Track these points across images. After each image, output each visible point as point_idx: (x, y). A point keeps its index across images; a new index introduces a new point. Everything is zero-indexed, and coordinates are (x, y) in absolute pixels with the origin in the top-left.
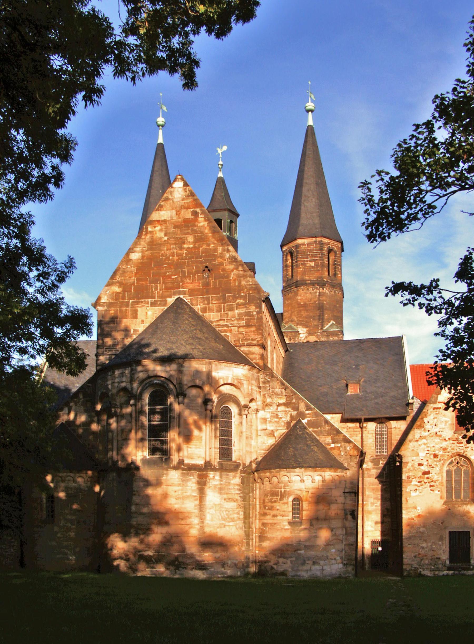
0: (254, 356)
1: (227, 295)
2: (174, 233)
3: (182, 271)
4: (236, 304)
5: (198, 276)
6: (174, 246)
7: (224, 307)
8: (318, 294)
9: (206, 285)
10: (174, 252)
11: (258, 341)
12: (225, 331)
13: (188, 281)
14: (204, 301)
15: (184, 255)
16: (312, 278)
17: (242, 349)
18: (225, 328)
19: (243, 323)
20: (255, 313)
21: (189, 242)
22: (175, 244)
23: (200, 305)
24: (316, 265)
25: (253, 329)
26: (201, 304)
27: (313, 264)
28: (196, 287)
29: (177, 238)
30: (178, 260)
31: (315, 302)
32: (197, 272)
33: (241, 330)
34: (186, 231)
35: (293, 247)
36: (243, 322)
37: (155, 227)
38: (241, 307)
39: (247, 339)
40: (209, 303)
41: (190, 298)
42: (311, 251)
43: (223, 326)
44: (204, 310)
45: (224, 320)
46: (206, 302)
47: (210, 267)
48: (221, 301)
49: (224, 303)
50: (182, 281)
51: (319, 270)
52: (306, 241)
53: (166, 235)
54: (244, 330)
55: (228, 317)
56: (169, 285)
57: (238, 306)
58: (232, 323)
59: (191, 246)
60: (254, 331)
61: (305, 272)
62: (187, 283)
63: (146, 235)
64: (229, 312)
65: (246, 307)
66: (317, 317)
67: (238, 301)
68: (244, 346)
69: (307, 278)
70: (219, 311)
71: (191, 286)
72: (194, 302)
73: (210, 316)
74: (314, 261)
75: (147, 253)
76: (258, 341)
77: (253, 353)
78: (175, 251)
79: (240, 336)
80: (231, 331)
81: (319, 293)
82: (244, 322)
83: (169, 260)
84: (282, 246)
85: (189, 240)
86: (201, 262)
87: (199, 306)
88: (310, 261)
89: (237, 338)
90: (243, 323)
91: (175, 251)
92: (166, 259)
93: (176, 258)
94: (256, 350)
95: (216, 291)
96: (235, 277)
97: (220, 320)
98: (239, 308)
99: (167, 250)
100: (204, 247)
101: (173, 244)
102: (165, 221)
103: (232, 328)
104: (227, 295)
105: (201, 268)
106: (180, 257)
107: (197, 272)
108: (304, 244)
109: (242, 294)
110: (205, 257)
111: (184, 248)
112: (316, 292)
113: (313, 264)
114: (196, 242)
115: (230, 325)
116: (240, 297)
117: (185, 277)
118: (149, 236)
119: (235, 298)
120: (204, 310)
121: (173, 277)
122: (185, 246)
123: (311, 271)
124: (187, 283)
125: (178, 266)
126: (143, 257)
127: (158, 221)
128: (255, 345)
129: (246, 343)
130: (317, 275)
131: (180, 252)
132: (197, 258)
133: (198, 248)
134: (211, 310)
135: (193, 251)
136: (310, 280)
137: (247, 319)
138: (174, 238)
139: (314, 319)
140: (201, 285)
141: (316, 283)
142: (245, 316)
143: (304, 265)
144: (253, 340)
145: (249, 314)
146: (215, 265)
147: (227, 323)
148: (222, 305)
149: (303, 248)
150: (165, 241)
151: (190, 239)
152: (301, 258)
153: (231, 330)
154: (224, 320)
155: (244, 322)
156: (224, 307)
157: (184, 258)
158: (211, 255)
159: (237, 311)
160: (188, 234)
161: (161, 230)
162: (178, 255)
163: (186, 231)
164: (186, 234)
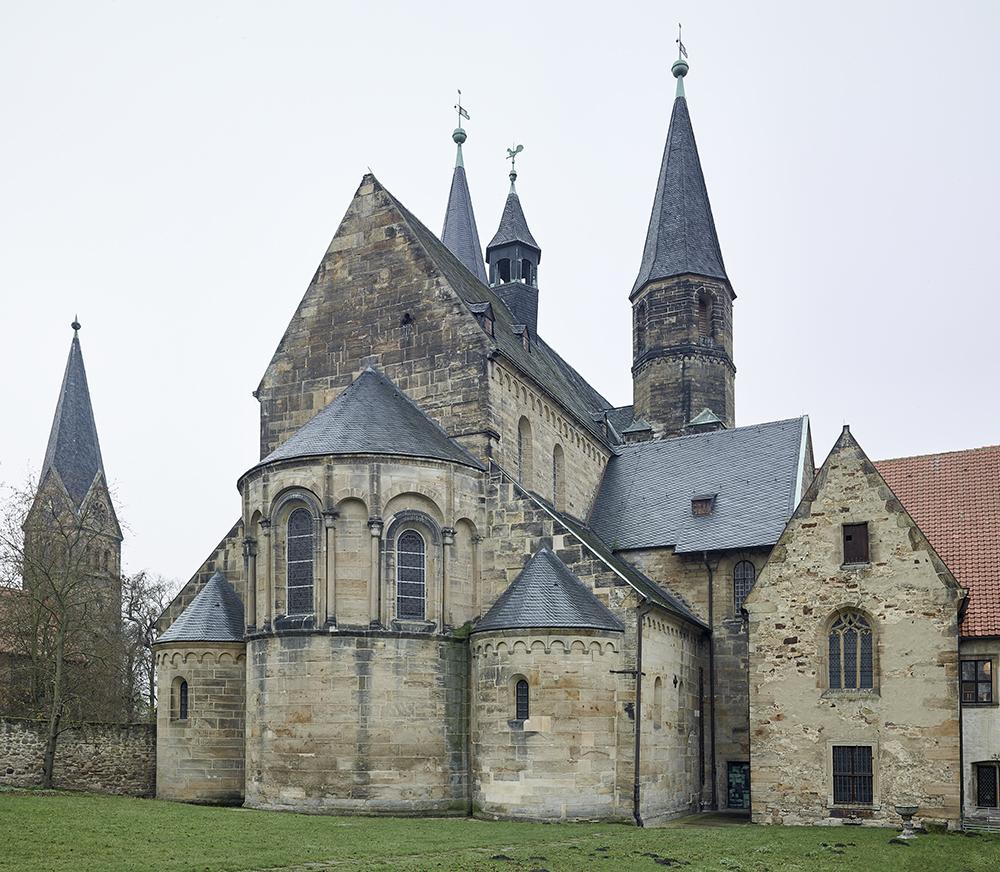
0: (475, 450)
2: (363, 268)
7: (432, 375)
9: (407, 343)
12: (434, 414)
13: (382, 341)
15: (375, 302)
17: (458, 440)
18: (434, 410)
19: (459, 399)
20: (476, 381)
25: (474, 406)
32: (393, 326)
33: (457, 409)
34: (379, 263)
37: (335, 263)
39: (463, 425)
40: (411, 373)
43: (431, 407)
44: (404, 384)
45: (432, 396)
46: (406, 371)
47: (413, 314)
48: (428, 367)
50: (372, 343)
53: (350, 274)
56: (356, 351)
58: (443, 400)
59: (386, 284)
60: (475, 411)
63: (323, 276)
64: (439, 384)
68: (460, 436)
71: (385, 349)
73: (412, 393)
75: (325, 305)
79: (455, 420)
86: (399, 309)
87: (397, 379)
90: (459, 398)
93: (364, 307)
94: (479, 440)
98: (454, 375)
102: (348, 251)
107: (393, 326)
116: (454, 357)
117: (376, 335)
118: (327, 278)
119: (448, 359)
120: (404, 384)
122: (377, 286)
125: (368, 319)
126: (319, 312)
127: (340, 252)
128: (477, 433)
134: (413, 383)
137: (466, 392)
144: (474, 424)
145: (468, 383)
151: (385, 274)
153: (442, 412)
156: (432, 375)
158: (413, 297)
159: (449, 381)
161: (343, 267)
162: (367, 303)
163: (379, 263)
164: (379, 268)
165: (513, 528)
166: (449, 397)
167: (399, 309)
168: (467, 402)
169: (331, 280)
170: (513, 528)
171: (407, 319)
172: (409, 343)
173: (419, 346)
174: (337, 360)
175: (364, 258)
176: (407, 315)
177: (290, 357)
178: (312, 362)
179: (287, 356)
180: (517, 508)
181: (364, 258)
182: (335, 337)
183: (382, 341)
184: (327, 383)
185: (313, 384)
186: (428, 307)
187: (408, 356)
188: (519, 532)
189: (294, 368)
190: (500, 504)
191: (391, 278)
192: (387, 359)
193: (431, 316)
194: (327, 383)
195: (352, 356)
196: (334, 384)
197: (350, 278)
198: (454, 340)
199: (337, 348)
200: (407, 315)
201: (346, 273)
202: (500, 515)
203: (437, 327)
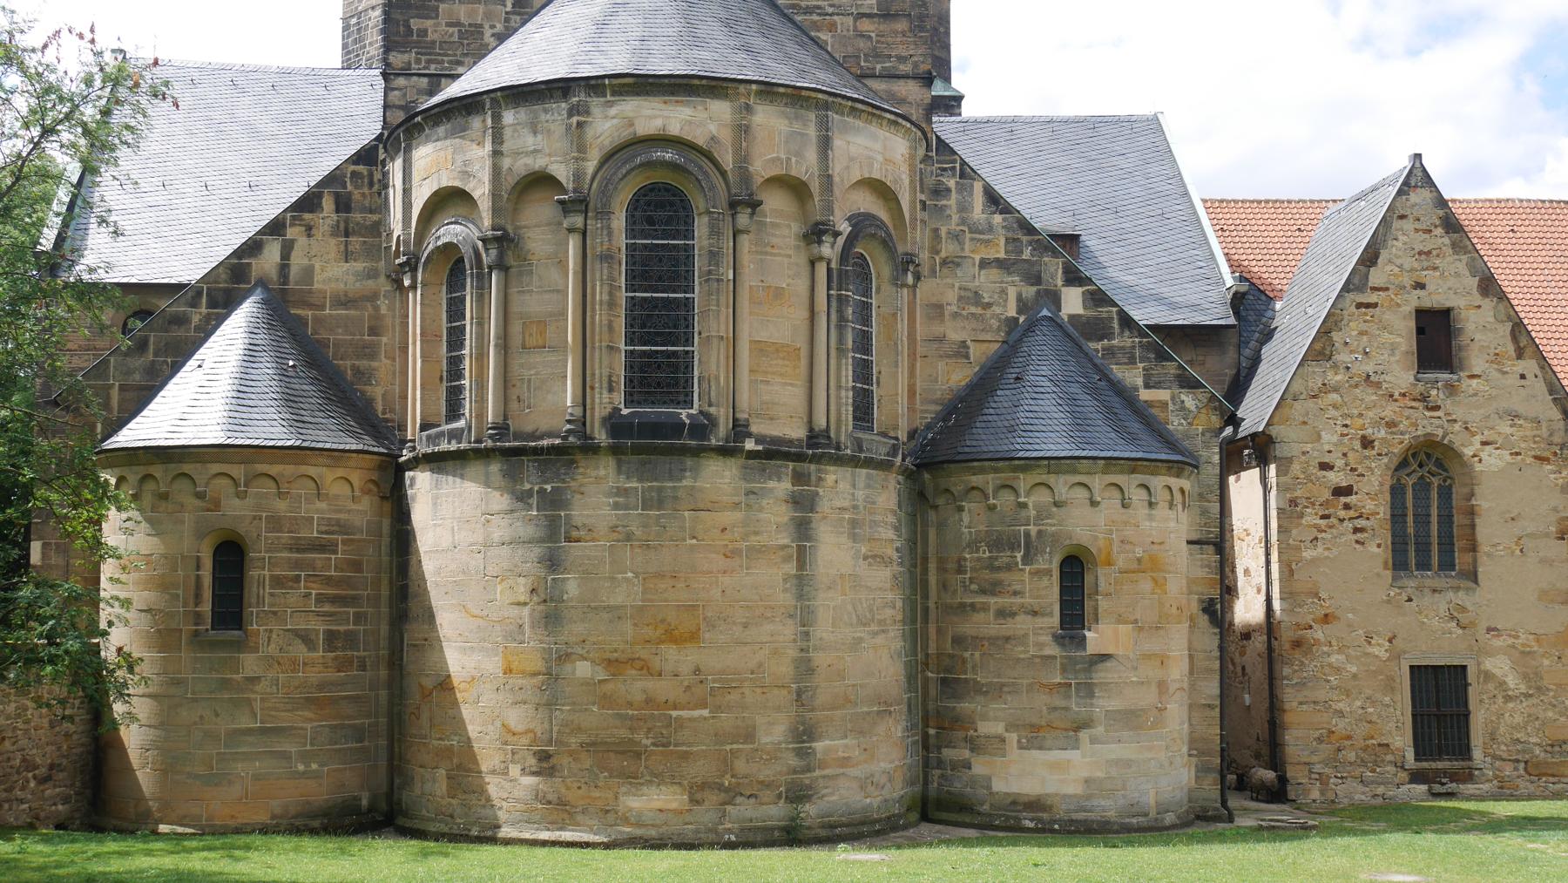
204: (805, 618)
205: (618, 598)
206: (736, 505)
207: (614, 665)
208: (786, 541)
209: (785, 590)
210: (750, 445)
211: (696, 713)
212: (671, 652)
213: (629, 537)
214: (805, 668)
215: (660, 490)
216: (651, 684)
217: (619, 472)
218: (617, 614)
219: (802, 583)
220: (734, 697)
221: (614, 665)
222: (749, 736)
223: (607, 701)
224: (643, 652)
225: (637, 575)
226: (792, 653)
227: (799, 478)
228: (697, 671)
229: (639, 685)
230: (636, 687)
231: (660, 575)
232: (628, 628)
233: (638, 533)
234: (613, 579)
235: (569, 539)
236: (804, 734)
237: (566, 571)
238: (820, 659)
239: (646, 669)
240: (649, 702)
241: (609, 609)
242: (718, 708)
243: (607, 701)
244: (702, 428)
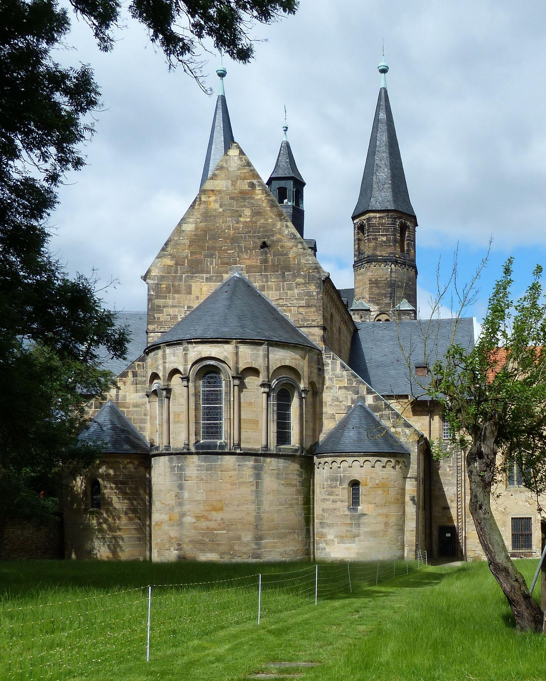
1: (286, 273)
2: (231, 205)
3: (238, 246)
4: (296, 283)
5: (255, 251)
6: (230, 219)
7: (283, 285)
8: (390, 270)
9: (265, 261)
10: (230, 226)
11: (318, 322)
13: (246, 257)
14: (263, 278)
16: (384, 254)
17: (302, 329)
18: (285, 308)
19: (303, 303)
20: (315, 293)
21: (246, 215)
22: (231, 217)
23: (258, 283)
24: (388, 240)
25: (313, 309)
26: (259, 282)
27: (384, 239)
28: (254, 263)
29: (233, 210)
30: (234, 233)
31: (387, 278)
32: (254, 248)
33: (301, 310)
34: (243, 204)
35: (364, 220)
36: (302, 302)
38: (300, 286)
40: (267, 281)
41: (247, 275)
42: (382, 224)
43: (282, 306)
44: (263, 288)
45: (283, 299)
46: (264, 280)
47: (269, 243)
48: (280, 279)
49: (283, 282)
50: (238, 257)
51: (391, 246)
52: (378, 215)
54: (303, 310)
55: (287, 296)
56: (226, 260)
57: (298, 284)
58: (292, 302)
59: (249, 219)
60: (314, 312)
61: (376, 246)
62: (245, 259)
64: (289, 292)
65: (305, 286)
66: (389, 295)
67: (298, 280)
69: (378, 253)
70: (278, 289)
71: (248, 262)
72: (252, 279)
73: (268, 294)
74: (386, 235)
76: (318, 322)
77: (313, 335)
78: (231, 225)
79: (300, 316)
80: (290, 311)
81: (391, 269)
82: (304, 302)
83: (225, 233)
84: (354, 218)
85: (245, 214)
86: (259, 238)
88: (382, 235)
89: (296, 318)
90: (303, 303)
91: (231, 225)
92: (222, 232)
93: (232, 232)
95: (275, 268)
96: (294, 255)
97: (279, 299)
98: (299, 288)
99: (223, 223)
100: (262, 221)
101: (229, 217)
103: (291, 308)
104: (286, 273)
105: (259, 243)
106: (237, 231)
107: (254, 248)
108: (375, 218)
109: (302, 273)
110: (263, 231)
111: (241, 222)
112: (388, 269)
113: (384, 239)
114: (253, 216)
115: (290, 305)
116: (299, 276)
119: (294, 276)
120: (263, 288)
121: (229, 252)
122: (241, 219)
123: (383, 246)
124: (245, 259)
125: (234, 240)
129: (305, 323)
130: (390, 250)
131: (236, 225)
132: (254, 233)
133: (256, 223)
134: (270, 288)
135: (251, 225)
136: (382, 256)
137: (307, 299)
138: (230, 210)
139: (386, 297)
140: (258, 261)
141: (388, 259)
142: (305, 296)
143: (376, 239)
144: (313, 321)
145: (309, 294)
146: (273, 241)
147: (286, 303)
148: (281, 283)
149: (374, 221)
150: (220, 213)
151: (247, 212)
152: (373, 232)
153: (291, 310)
154: (283, 299)
155: (304, 302)
156: (283, 285)
157: (240, 232)
160: (245, 206)
162: (234, 229)
163: (243, 204)
165: (340, 388)
166: (295, 301)
167: (259, 238)
168: (308, 306)
169: (206, 209)
170: (340, 388)
171: (264, 245)
172: (265, 261)
173: (273, 265)
174: (211, 263)
175: (232, 198)
176: (264, 243)
177: (173, 256)
178: (191, 263)
179: (170, 255)
180: (342, 376)
181: (232, 198)
182: (209, 248)
183: (246, 257)
184: (203, 279)
185: (192, 278)
186: (280, 241)
187: (266, 270)
188: (343, 391)
189: (177, 264)
190: (331, 373)
191: (252, 216)
192: (249, 269)
193: (282, 247)
194: (203, 279)
195: (223, 263)
196: (208, 280)
197: (221, 210)
198: (298, 264)
199: (211, 256)
200: (264, 243)
201: (217, 206)
202: (331, 379)
203: (287, 254)
204: (259, 503)
205: (199, 498)
206: (235, 470)
207: (198, 518)
208: (252, 480)
209: (252, 495)
210: (238, 451)
211: (222, 532)
212: (214, 514)
213: (202, 480)
214: (258, 518)
215: (211, 465)
216: (208, 523)
217: (199, 460)
218: (198, 502)
219: (258, 492)
220: (234, 527)
221: (198, 518)
222: (239, 538)
223: (196, 528)
224: (206, 514)
225: (204, 491)
226: (254, 514)
227: (256, 461)
228: (222, 519)
229: (205, 523)
230: (204, 524)
231: (211, 491)
232: (202, 507)
233: (204, 478)
234: (197, 492)
235: (185, 480)
236: (258, 538)
237: (184, 490)
238: (264, 516)
239: (207, 519)
240: (208, 528)
241: (196, 501)
242: (229, 530)
243: (196, 528)
244: (222, 447)
